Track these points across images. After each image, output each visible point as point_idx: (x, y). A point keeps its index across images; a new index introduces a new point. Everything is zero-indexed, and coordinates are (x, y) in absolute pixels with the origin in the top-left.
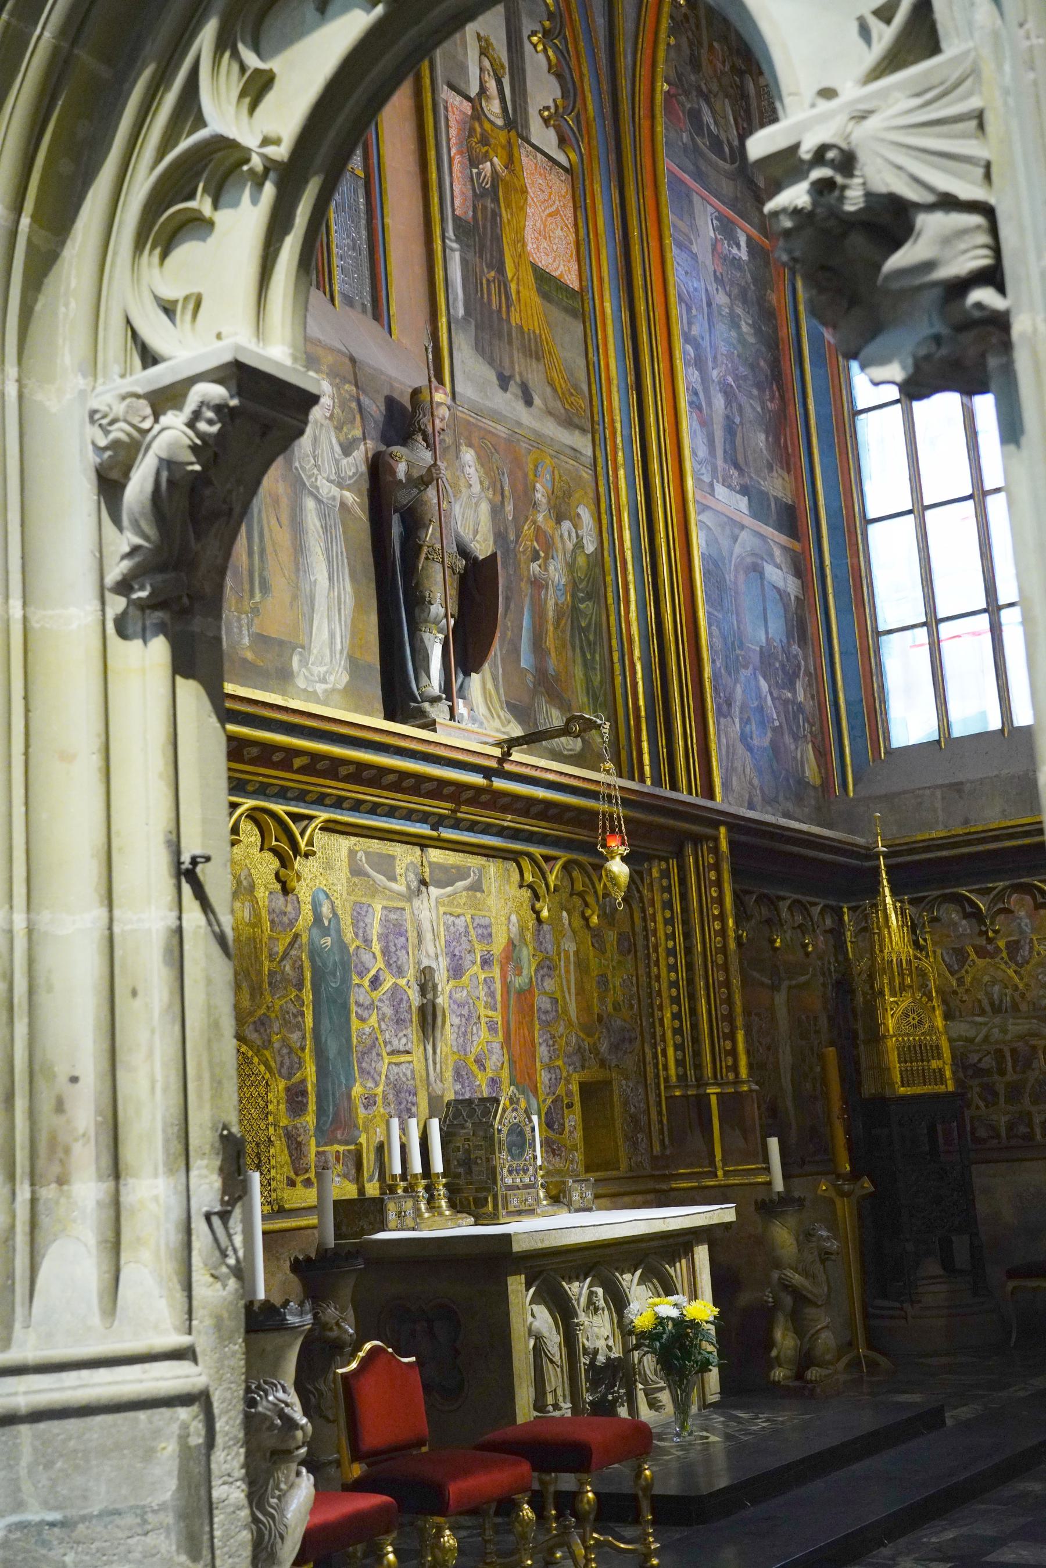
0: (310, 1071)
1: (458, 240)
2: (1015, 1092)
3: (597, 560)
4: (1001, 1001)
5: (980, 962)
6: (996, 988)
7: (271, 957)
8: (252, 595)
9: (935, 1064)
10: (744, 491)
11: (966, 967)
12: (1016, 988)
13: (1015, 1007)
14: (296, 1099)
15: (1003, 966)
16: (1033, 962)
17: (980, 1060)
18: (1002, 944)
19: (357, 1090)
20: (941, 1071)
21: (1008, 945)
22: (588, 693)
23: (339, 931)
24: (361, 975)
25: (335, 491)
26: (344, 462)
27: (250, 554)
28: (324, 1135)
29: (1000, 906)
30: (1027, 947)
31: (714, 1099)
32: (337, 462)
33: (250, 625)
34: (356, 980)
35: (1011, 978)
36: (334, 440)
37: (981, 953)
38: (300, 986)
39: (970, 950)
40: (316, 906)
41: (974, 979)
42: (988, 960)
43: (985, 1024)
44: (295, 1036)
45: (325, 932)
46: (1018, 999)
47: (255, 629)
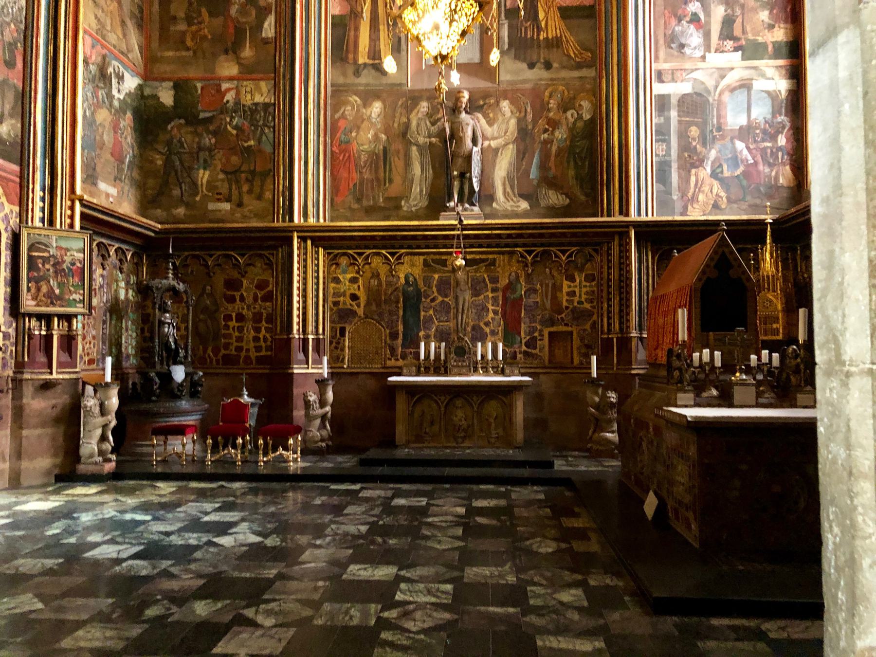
0: (401, 328)
1: (506, 18)
3: (592, 120)
7: (385, 294)
8: (385, 184)
9: (775, 326)
10: (736, 49)
14: (394, 336)
19: (422, 334)
20: (778, 329)
22: (576, 179)
23: (417, 285)
24: (426, 298)
25: (427, 140)
26: (433, 128)
27: (385, 172)
28: (403, 346)
31: (615, 340)
32: (429, 130)
33: (383, 194)
34: (423, 299)
36: (428, 122)
38: (398, 302)
40: (407, 278)
44: (395, 317)
45: (410, 285)
47: (386, 195)
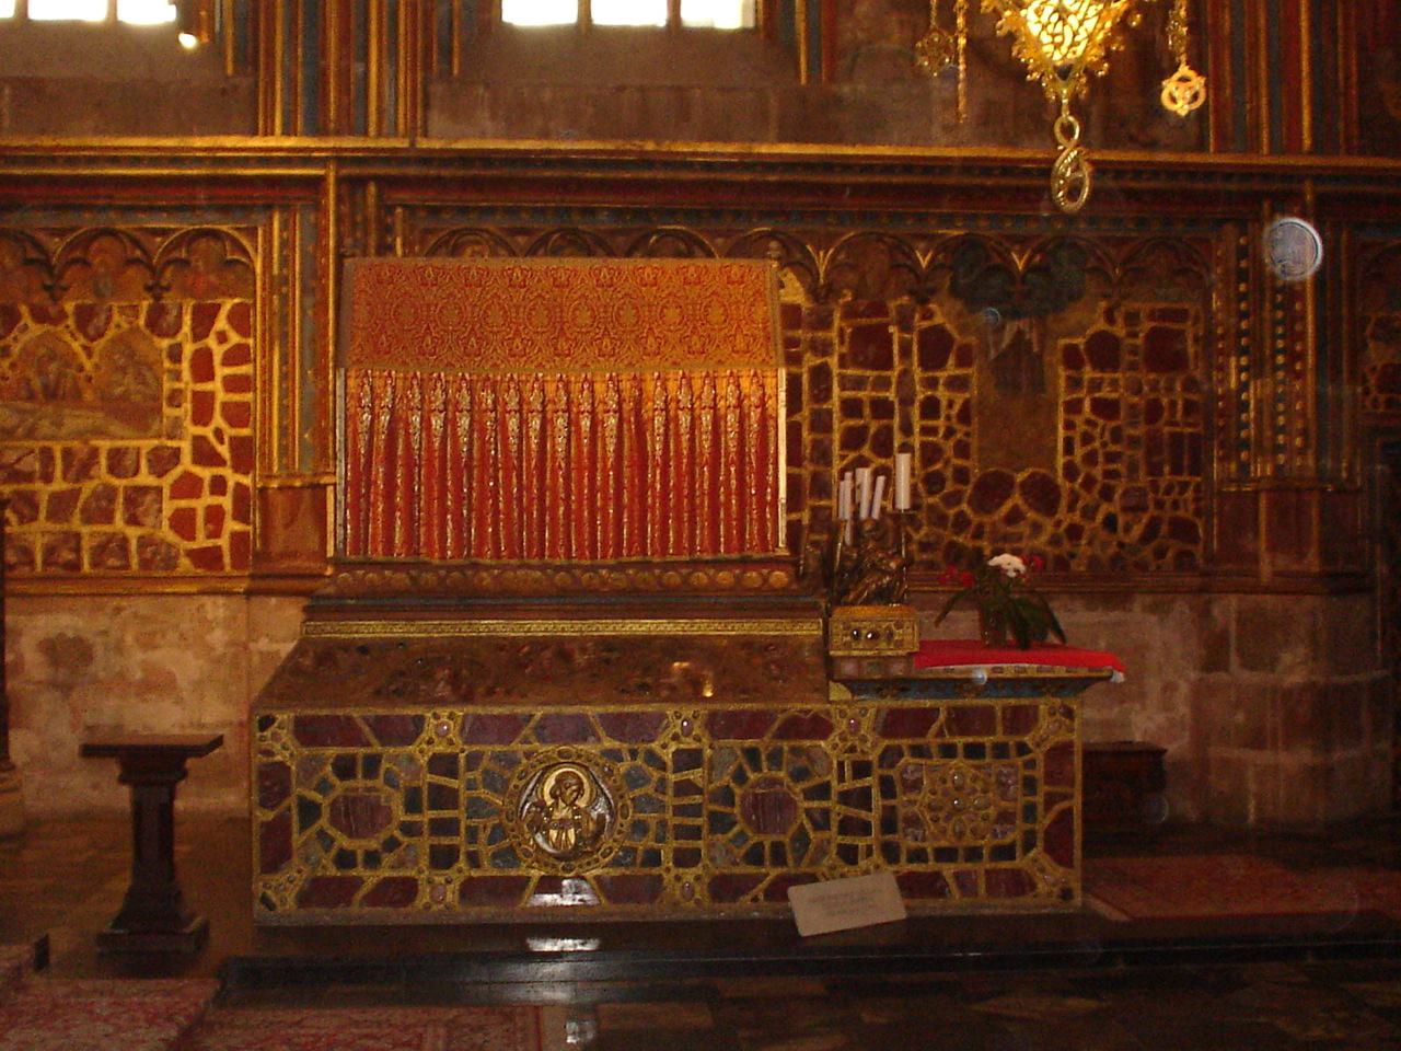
2: (61, 506)
4: (57, 387)
5: (36, 330)
6: (53, 367)
11: (15, 332)
12: (81, 369)
13: (77, 394)
15: (68, 338)
16: (111, 333)
17: (19, 460)
18: (69, 307)
21: (79, 310)
29: (78, 254)
30: (103, 317)
35: (75, 354)
37: (40, 316)
39: (24, 309)
41: (24, 350)
42: (47, 327)
43: (32, 412)
46: (82, 384)
